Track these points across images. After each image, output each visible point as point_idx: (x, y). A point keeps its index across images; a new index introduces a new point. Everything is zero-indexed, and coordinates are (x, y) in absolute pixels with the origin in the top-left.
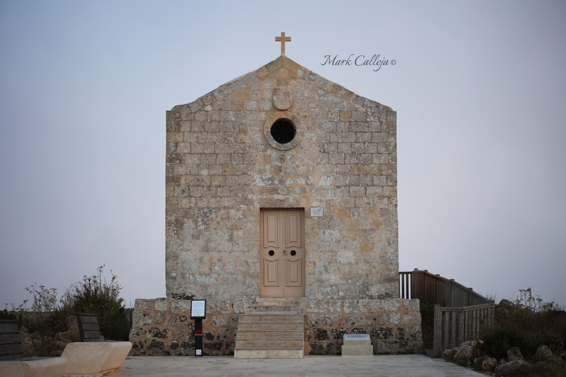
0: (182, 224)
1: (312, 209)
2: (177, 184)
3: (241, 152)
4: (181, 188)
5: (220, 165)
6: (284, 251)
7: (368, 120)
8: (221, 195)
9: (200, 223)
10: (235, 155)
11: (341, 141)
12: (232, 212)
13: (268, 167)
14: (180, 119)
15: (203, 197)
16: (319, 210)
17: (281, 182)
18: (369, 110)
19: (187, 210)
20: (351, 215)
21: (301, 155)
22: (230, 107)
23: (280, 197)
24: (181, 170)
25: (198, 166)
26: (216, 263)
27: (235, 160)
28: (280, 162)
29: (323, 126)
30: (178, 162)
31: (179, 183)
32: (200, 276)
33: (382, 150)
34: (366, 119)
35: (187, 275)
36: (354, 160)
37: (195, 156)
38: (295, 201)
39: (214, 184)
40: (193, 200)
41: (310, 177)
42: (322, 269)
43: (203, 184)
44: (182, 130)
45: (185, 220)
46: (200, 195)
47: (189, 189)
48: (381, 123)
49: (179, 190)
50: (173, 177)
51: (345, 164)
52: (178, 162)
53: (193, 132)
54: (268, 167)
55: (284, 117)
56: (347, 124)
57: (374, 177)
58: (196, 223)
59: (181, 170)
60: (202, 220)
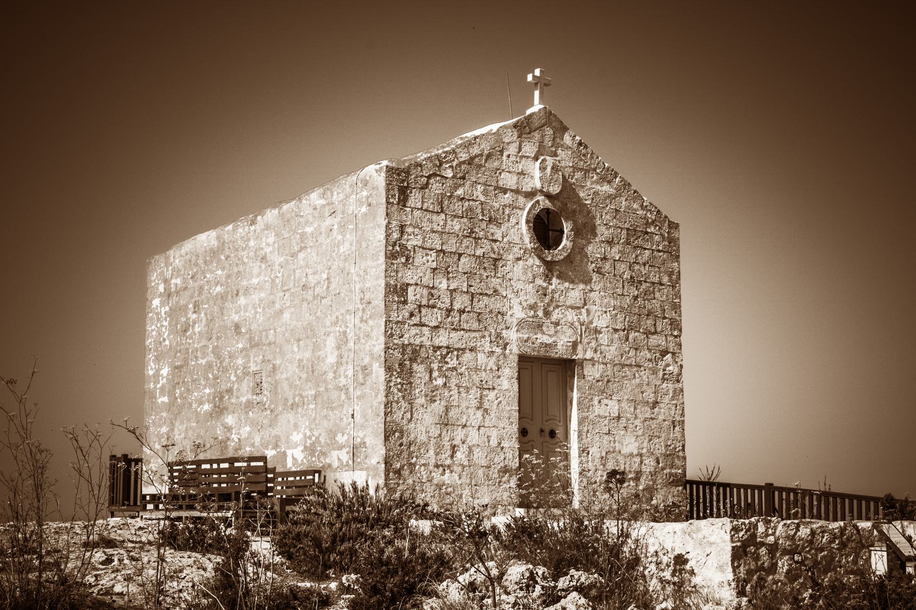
0: (411, 372)
1: (585, 362)
2: (403, 299)
3: (493, 256)
5: (465, 273)
11: (617, 258)
14: (405, 184)
15: (440, 328)
17: (547, 314)
19: (418, 348)
21: (570, 273)
24: (409, 276)
25: (434, 272)
26: (458, 446)
28: (545, 281)
30: (403, 260)
31: (404, 298)
32: (436, 469)
34: (646, 228)
35: (417, 467)
38: (564, 347)
39: (457, 306)
45: (415, 366)
47: (420, 312)
50: (396, 285)
51: (623, 295)
53: (426, 210)
58: (431, 372)
59: (409, 276)
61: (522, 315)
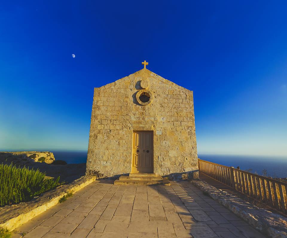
0: (97, 137)
4: (98, 120)
6: (144, 151)
7: (181, 94)
8: (116, 124)
9: (105, 136)
10: (123, 107)
12: (121, 132)
13: (137, 112)
16: (160, 132)
17: (143, 119)
18: (181, 90)
20: (175, 134)
22: (122, 87)
23: (143, 126)
27: (123, 109)
29: (162, 96)
30: (98, 109)
33: (187, 106)
36: (175, 110)
37: (106, 106)
40: (103, 126)
41: (156, 117)
42: (162, 160)
43: (108, 119)
44: (101, 95)
45: (99, 134)
46: (106, 124)
48: (186, 95)
49: (96, 121)
52: (98, 109)
54: (137, 112)
55: (145, 91)
56: (172, 95)
57: (185, 118)
58: (103, 136)
60: (107, 135)
61: (135, 120)
